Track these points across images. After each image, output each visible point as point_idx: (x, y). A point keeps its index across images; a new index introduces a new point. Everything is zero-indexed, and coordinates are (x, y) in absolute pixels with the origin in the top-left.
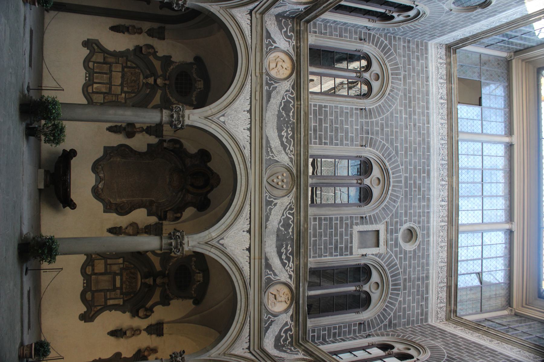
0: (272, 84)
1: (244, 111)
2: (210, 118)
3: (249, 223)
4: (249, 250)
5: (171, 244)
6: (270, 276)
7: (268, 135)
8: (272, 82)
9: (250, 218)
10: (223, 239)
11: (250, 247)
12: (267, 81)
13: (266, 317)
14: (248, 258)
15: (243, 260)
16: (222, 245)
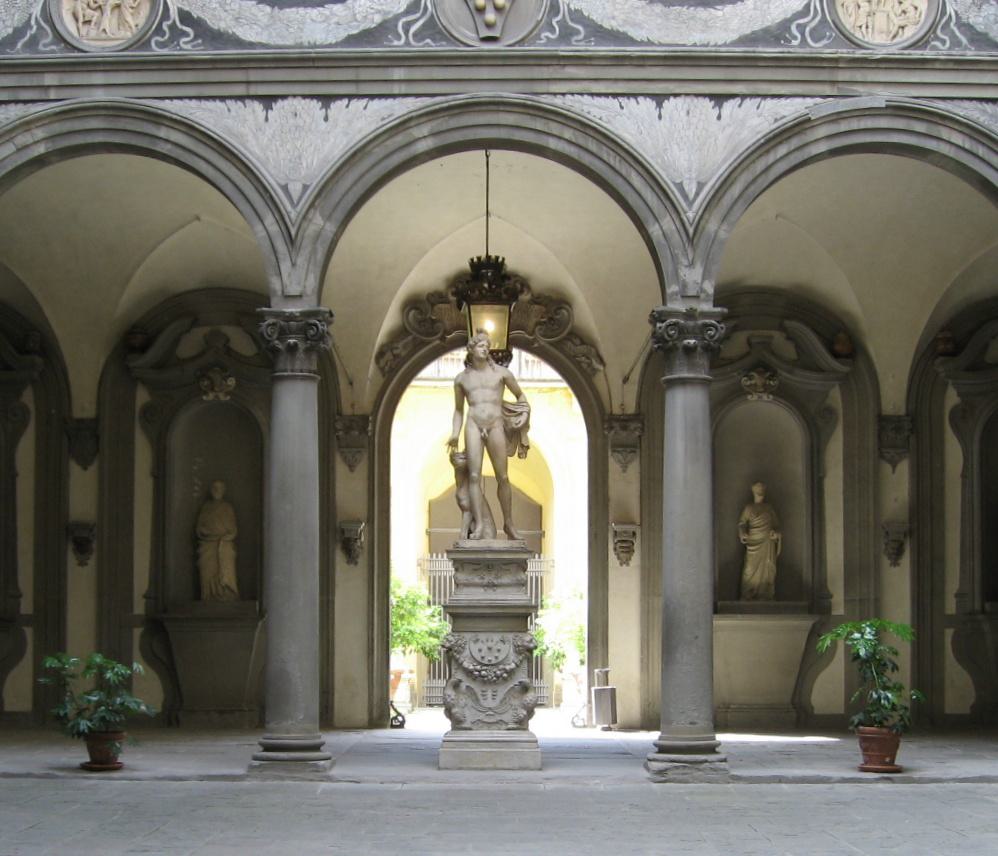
0: (173, 27)
1: (267, 119)
2: (293, 232)
3: (632, 100)
4: (719, 99)
5: (689, 350)
6: (808, 29)
7: (342, 35)
8: (165, 27)
9: (615, 95)
10: (680, 187)
11: (712, 96)
12: (158, 44)
13: (943, 42)
14: (748, 102)
15: (753, 119)
16: (700, 186)
